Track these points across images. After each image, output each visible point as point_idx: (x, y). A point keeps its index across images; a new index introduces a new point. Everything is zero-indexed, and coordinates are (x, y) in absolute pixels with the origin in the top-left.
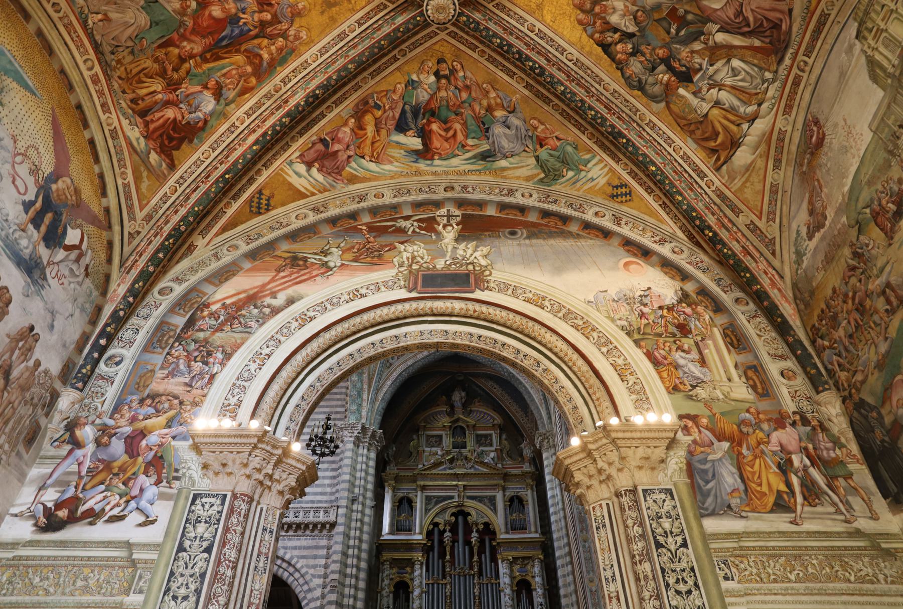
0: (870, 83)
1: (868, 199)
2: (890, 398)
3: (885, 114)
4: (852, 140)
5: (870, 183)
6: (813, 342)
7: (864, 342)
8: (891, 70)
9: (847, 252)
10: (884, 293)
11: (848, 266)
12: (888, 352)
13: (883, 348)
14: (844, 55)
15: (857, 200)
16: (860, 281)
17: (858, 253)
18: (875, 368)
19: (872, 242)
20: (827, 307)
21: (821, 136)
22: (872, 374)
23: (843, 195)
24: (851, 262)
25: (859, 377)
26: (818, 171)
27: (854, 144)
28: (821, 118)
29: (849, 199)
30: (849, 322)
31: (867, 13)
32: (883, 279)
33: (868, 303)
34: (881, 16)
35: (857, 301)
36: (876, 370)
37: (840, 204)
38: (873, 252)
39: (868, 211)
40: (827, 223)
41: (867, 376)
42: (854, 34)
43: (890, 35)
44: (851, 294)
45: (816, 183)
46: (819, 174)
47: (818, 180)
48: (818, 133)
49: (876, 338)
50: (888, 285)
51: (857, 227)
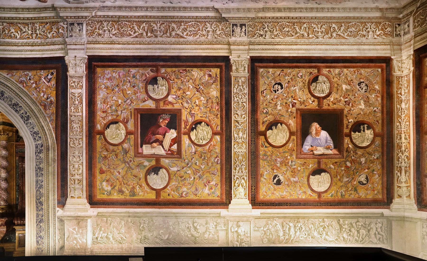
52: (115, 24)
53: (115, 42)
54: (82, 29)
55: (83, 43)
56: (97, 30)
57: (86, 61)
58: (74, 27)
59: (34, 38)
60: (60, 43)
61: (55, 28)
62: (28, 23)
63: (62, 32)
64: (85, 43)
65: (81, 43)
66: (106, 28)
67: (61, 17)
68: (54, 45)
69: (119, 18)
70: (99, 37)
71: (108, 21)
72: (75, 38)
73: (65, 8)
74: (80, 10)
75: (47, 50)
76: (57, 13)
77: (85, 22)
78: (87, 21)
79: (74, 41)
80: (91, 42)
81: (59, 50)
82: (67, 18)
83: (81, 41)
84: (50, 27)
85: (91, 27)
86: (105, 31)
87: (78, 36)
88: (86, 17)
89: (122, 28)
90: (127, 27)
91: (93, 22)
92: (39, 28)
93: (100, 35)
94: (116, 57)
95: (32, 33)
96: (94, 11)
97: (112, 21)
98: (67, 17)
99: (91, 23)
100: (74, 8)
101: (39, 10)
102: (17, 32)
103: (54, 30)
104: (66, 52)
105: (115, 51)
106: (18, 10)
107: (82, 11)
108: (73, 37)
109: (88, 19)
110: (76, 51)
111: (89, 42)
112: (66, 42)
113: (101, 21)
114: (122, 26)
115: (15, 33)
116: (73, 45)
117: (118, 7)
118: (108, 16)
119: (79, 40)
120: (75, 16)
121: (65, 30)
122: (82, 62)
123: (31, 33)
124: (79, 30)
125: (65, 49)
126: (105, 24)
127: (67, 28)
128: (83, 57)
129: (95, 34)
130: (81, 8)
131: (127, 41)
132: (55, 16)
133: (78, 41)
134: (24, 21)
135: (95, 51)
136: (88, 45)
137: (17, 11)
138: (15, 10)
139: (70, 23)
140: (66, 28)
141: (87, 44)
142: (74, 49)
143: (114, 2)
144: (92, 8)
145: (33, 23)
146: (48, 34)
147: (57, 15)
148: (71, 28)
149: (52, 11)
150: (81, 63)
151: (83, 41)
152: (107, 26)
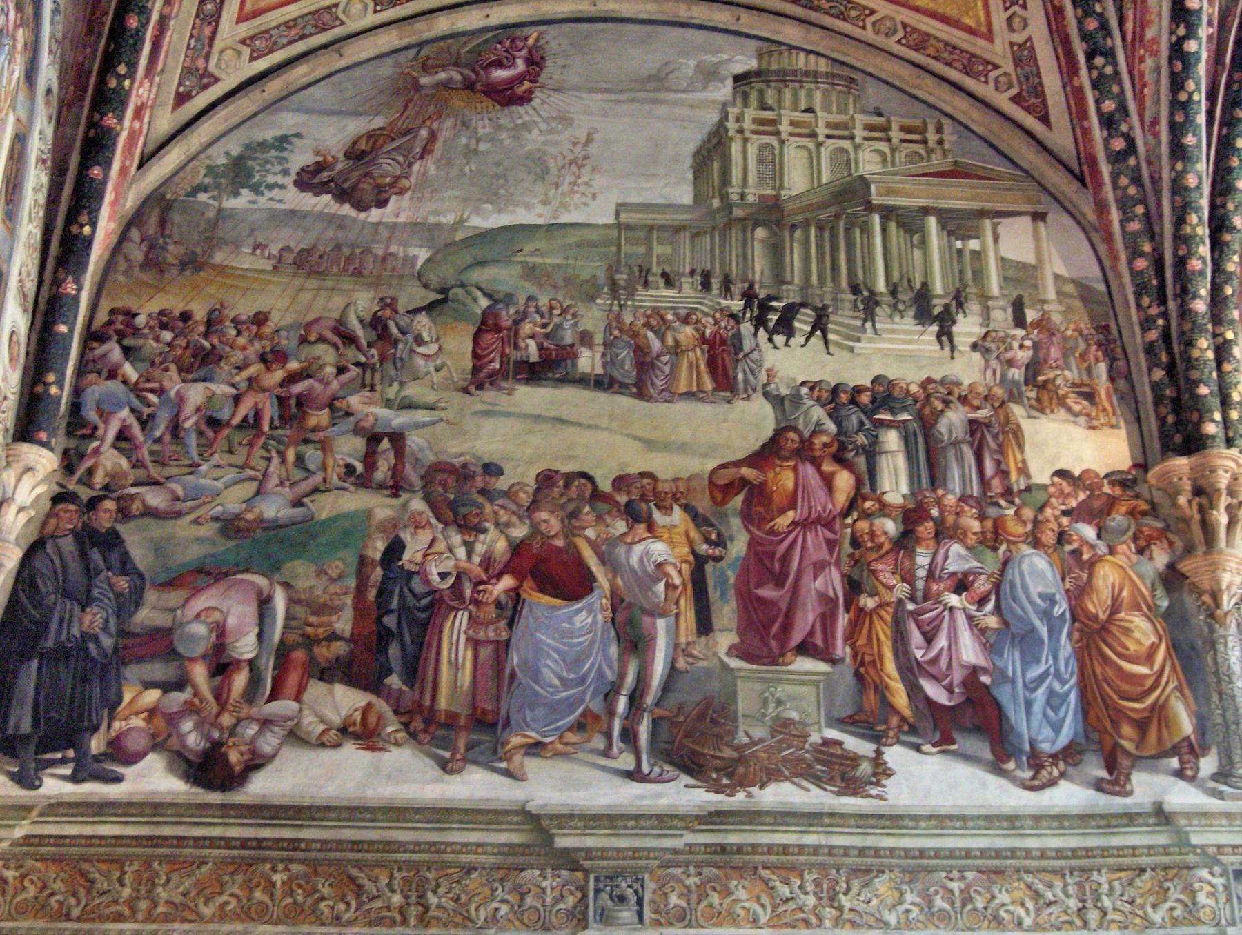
0: (688, 162)
1: (505, 288)
2: (197, 591)
3: (661, 228)
4: (569, 179)
5: (531, 272)
6: (93, 336)
7: (239, 459)
8: (734, 192)
9: (364, 302)
10: (374, 439)
11: (340, 321)
12: (275, 526)
13: (274, 508)
14: (692, 63)
15: (482, 263)
16: (341, 370)
17: (385, 328)
18: (216, 519)
19: (433, 348)
20: (209, 323)
21: (520, 90)
22: (197, 522)
23: (460, 223)
24: (354, 324)
25: (155, 498)
26: (449, 123)
27: (565, 187)
28: (550, 72)
29: (468, 242)
30: (237, 399)
31: (784, 77)
32: (398, 419)
33: (319, 417)
34: (797, 116)
35: (298, 388)
36: (217, 526)
37: (438, 226)
38: (420, 362)
39: (484, 303)
40: (375, 214)
41: (179, 515)
42: (739, 69)
43: (781, 155)
44: (294, 365)
45: (424, 133)
46: (446, 128)
47: (433, 136)
48: (520, 79)
49: (274, 480)
50: (397, 439)
51: (434, 296)
61: (1180, 887)
62: (1062, 868)
63: (1211, 902)
67: (1195, 847)
73: (1205, 814)
84: (1155, 883)
92: (1111, 889)
95: (1084, 907)
98: (1219, 847)
101: (1103, 822)
102: (1022, 904)
103: (1174, 894)
106: (1017, 824)
115: (1011, 908)
121: (1222, 898)
123: (1080, 905)
127: (1226, 888)
132: (1173, 845)
134: (1045, 863)
137: (1014, 828)
138: (1005, 824)
140: (1221, 889)
145: (1083, 870)
146: (1150, 910)
147: (1180, 840)
149: (1157, 828)
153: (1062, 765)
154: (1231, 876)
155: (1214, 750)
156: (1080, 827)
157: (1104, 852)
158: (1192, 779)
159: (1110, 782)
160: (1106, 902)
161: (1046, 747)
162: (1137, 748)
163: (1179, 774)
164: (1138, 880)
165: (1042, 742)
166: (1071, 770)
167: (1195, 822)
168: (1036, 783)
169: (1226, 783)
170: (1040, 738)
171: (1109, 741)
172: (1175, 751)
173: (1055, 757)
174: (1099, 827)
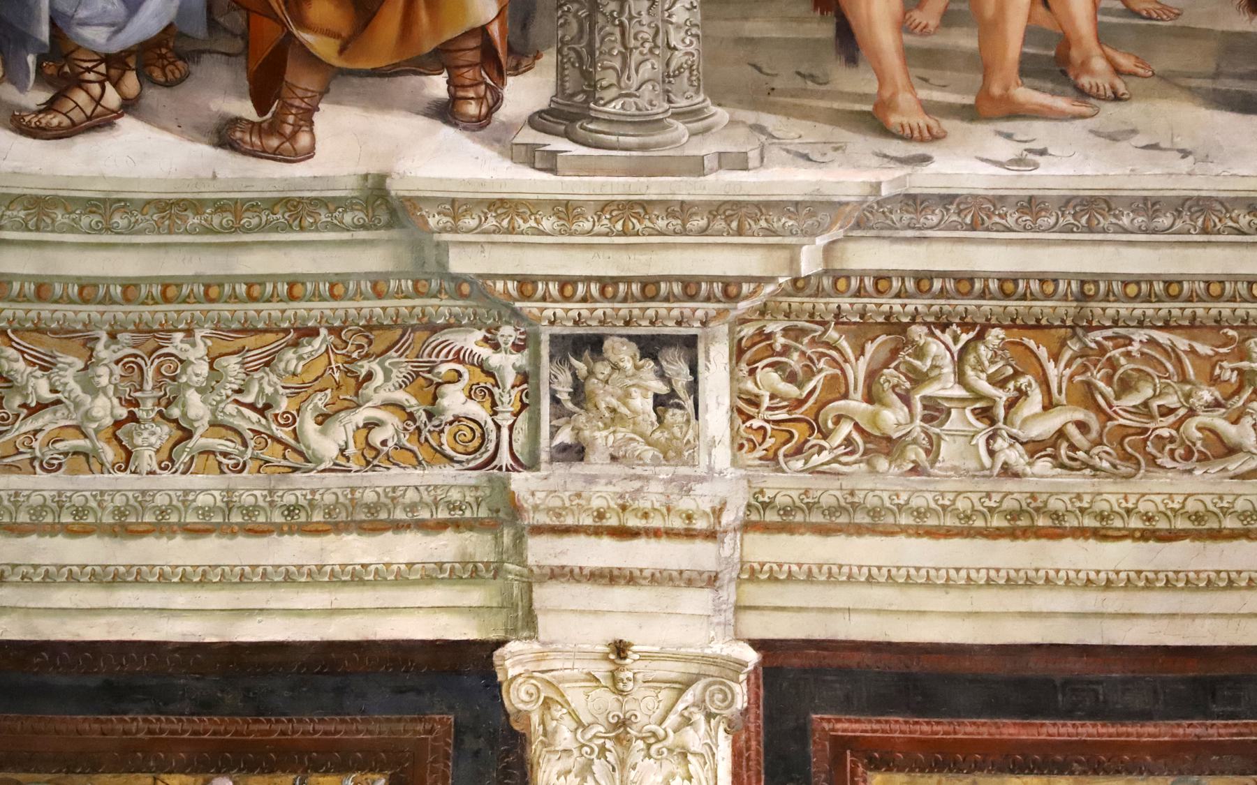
52: (1043, 352)
53: (1056, 515)
54: (693, 388)
55: (700, 524)
56: (856, 405)
57: (741, 702)
58: (602, 369)
59: (147, 459)
60: (443, 514)
61: (397, 376)
63: (477, 410)
64: (728, 518)
65: (678, 523)
66: (945, 387)
67: (458, 279)
68: (373, 527)
69: (1083, 297)
70: (882, 464)
71: (966, 326)
72: (616, 469)
74: (661, 224)
75: (289, 578)
76: (417, 247)
77: (721, 329)
78: (743, 321)
79: (602, 497)
80: (785, 511)
81: (433, 575)
82: (525, 297)
83: (686, 504)
85: (791, 378)
86: (935, 411)
87: (649, 453)
88: (730, 289)
89: (1126, 386)
90: (1184, 380)
91: (804, 332)
92: (215, 373)
93: (889, 445)
94: (1076, 666)
96: (812, 233)
97: (1013, 324)
98: (526, 284)
99: (780, 341)
100: (604, 207)
104: (508, 605)
105: (1064, 601)
107: (684, 232)
108: (597, 463)
109: (757, 302)
110: (620, 596)
111: (771, 517)
112: (515, 509)
113: (895, 327)
114: (1125, 366)
116: (597, 531)
117: (1066, 202)
118: (964, 282)
119: (655, 487)
120: (615, 281)
121: (509, 399)
122: (700, 704)
123: (123, 413)
124: (660, 402)
125: (497, 572)
126: (939, 349)
127: (524, 377)
128: (713, 661)
129: (838, 438)
130: (681, 210)
131: (1191, 506)
132: (399, 276)
133: (653, 495)
134: (45, 310)
135: (840, 597)
136: (753, 538)
139: (554, 339)
140: (510, 378)
141: (747, 526)
142: (609, 577)
143: (1019, 161)
144: (794, 207)
145: (144, 330)
146: (309, 426)
148: (565, 378)
149: (362, 235)
150: (687, 721)
151: (701, 500)
152: (960, 362)
153: (131, 82)
154: (545, 351)
155: (549, 59)
156: (157, 230)
157: (211, 289)
158: (480, 123)
159: (254, 127)
160: (196, 407)
161: (96, 37)
162: (342, 51)
163: (446, 112)
164: (290, 354)
165: (84, 23)
166: (154, 96)
167: (471, 222)
168: (55, 120)
169: (567, 135)
170: (82, 14)
171: (269, 34)
172: (441, 58)
173: (116, 63)
174: (210, 231)
